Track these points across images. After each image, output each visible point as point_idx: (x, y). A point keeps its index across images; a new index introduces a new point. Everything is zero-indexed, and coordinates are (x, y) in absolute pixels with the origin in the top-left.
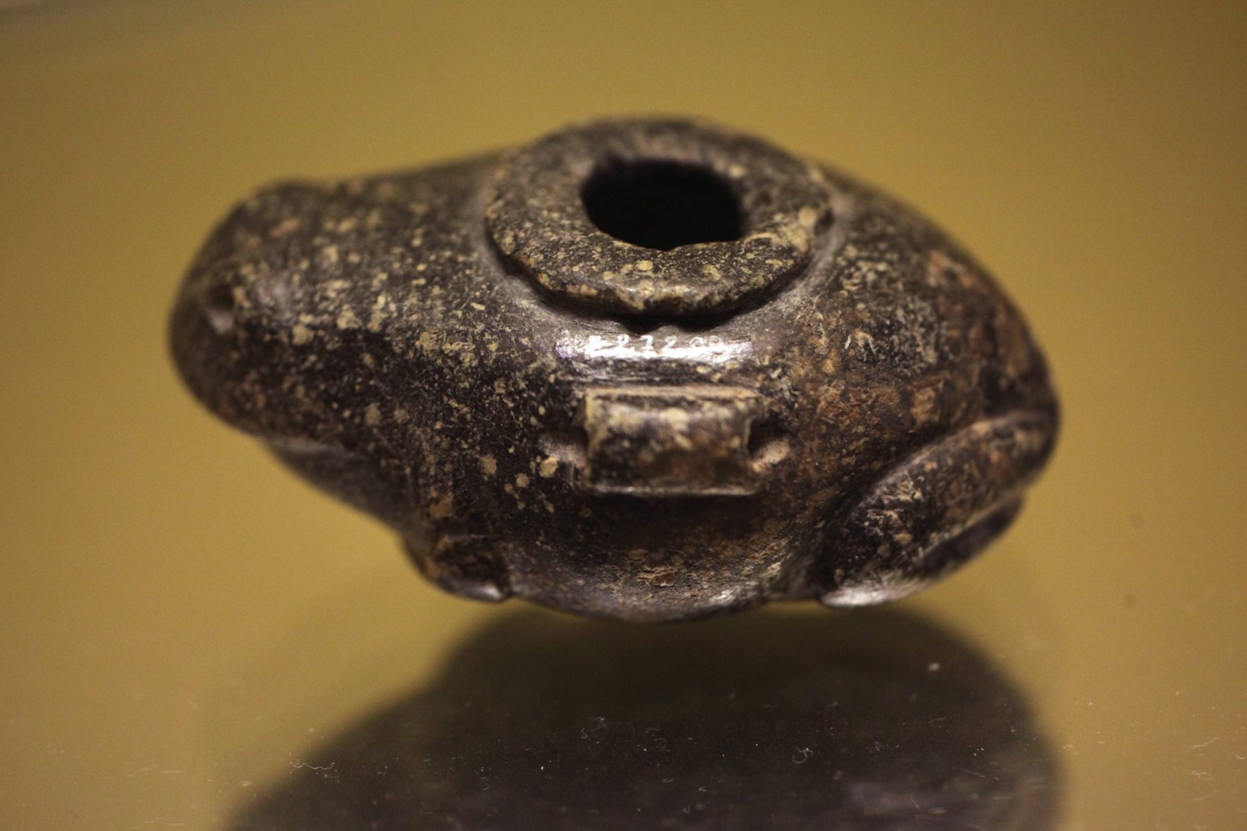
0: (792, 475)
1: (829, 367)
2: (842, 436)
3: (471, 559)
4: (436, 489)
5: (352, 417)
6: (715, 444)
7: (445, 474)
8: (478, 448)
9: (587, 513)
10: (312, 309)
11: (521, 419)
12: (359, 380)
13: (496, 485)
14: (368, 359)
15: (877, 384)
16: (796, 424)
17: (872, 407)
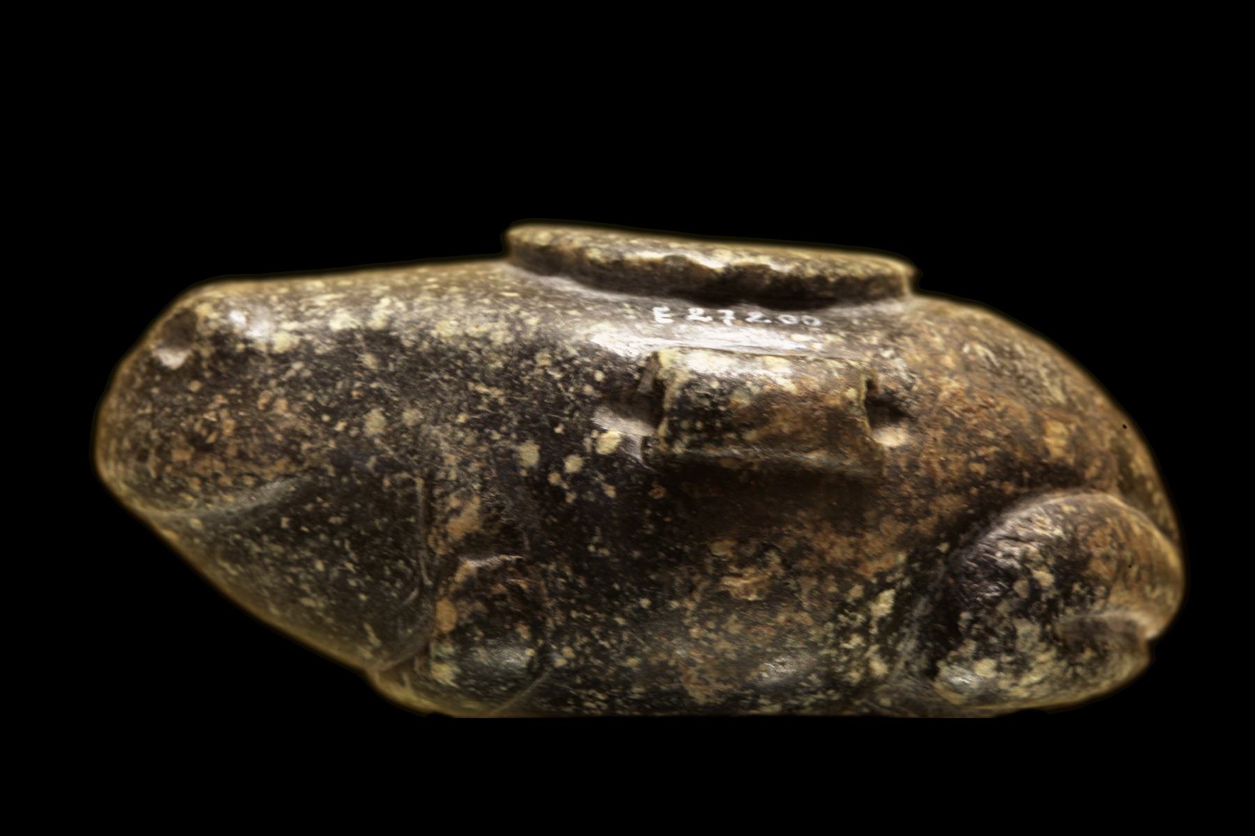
0: (913, 465)
1: (949, 361)
2: (970, 436)
3: (500, 588)
4: (457, 497)
5: (347, 429)
6: (825, 389)
7: (470, 475)
8: (514, 436)
9: (658, 493)
10: (297, 316)
11: (571, 389)
12: (358, 384)
13: (537, 480)
14: (369, 360)
15: (1004, 395)
16: (915, 407)
17: (1001, 415)
